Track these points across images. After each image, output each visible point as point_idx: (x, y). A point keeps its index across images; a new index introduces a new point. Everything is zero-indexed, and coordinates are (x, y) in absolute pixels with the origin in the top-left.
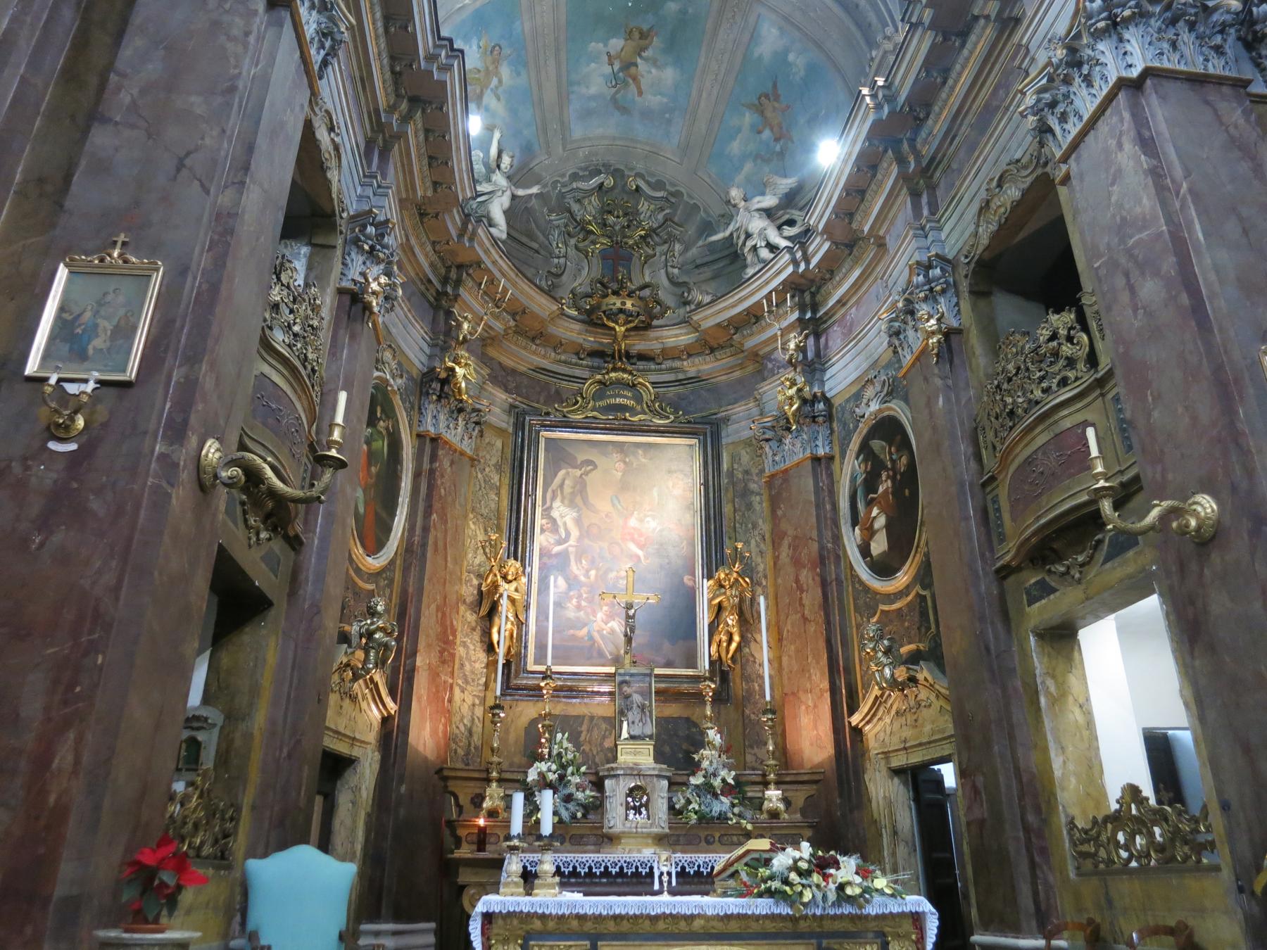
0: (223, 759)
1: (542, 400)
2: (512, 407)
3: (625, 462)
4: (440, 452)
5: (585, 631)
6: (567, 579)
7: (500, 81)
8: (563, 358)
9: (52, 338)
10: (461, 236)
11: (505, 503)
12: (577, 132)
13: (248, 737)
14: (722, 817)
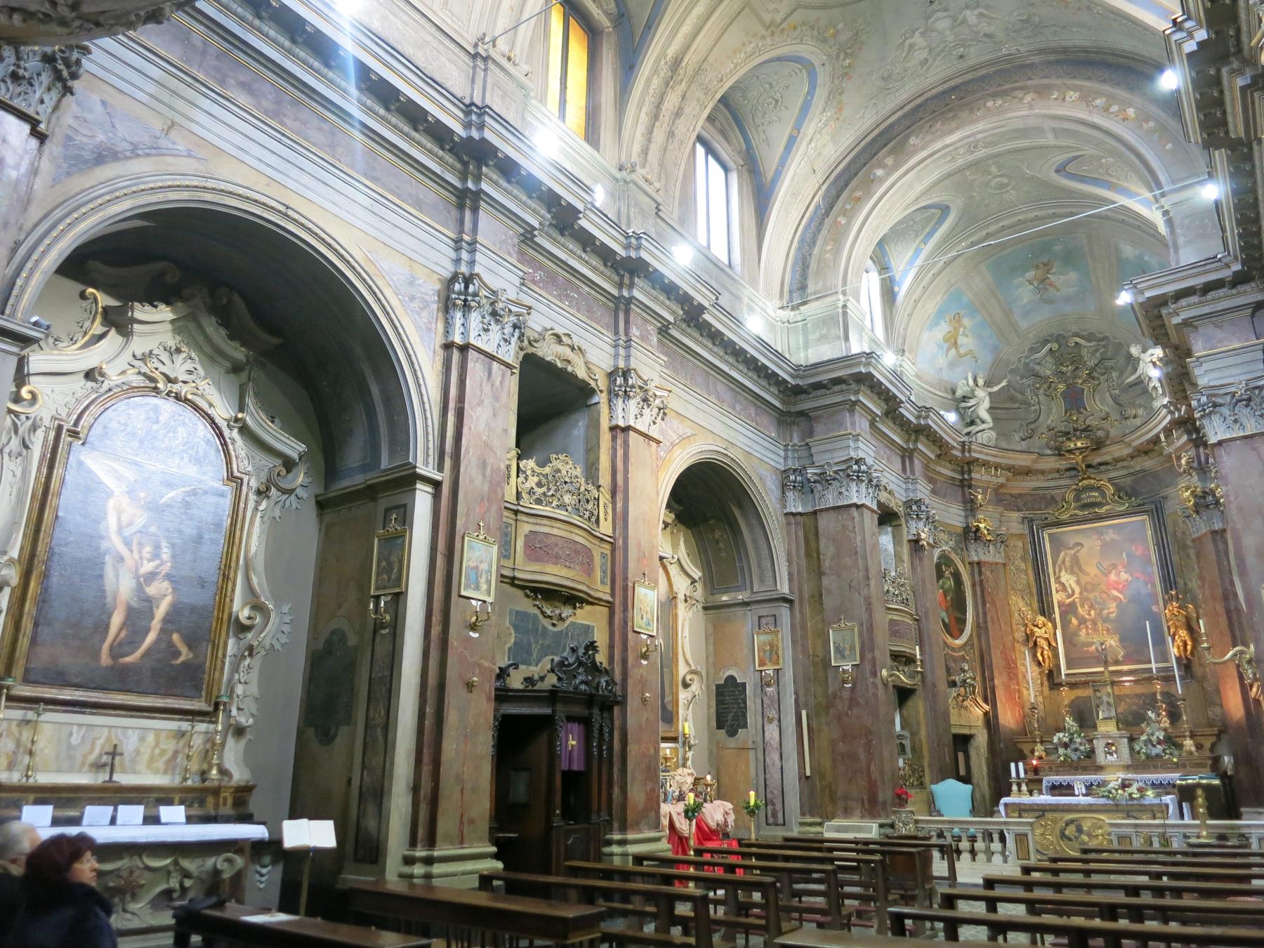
0: (913, 750)
1: (1043, 507)
2: (1024, 518)
3: (1099, 539)
4: (983, 569)
5: (1094, 647)
6: (1077, 618)
7: (965, 328)
8: (1050, 477)
9: (835, 653)
10: (963, 451)
11: (1032, 578)
12: (1024, 325)
13: (920, 740)
14: (1158, 756)
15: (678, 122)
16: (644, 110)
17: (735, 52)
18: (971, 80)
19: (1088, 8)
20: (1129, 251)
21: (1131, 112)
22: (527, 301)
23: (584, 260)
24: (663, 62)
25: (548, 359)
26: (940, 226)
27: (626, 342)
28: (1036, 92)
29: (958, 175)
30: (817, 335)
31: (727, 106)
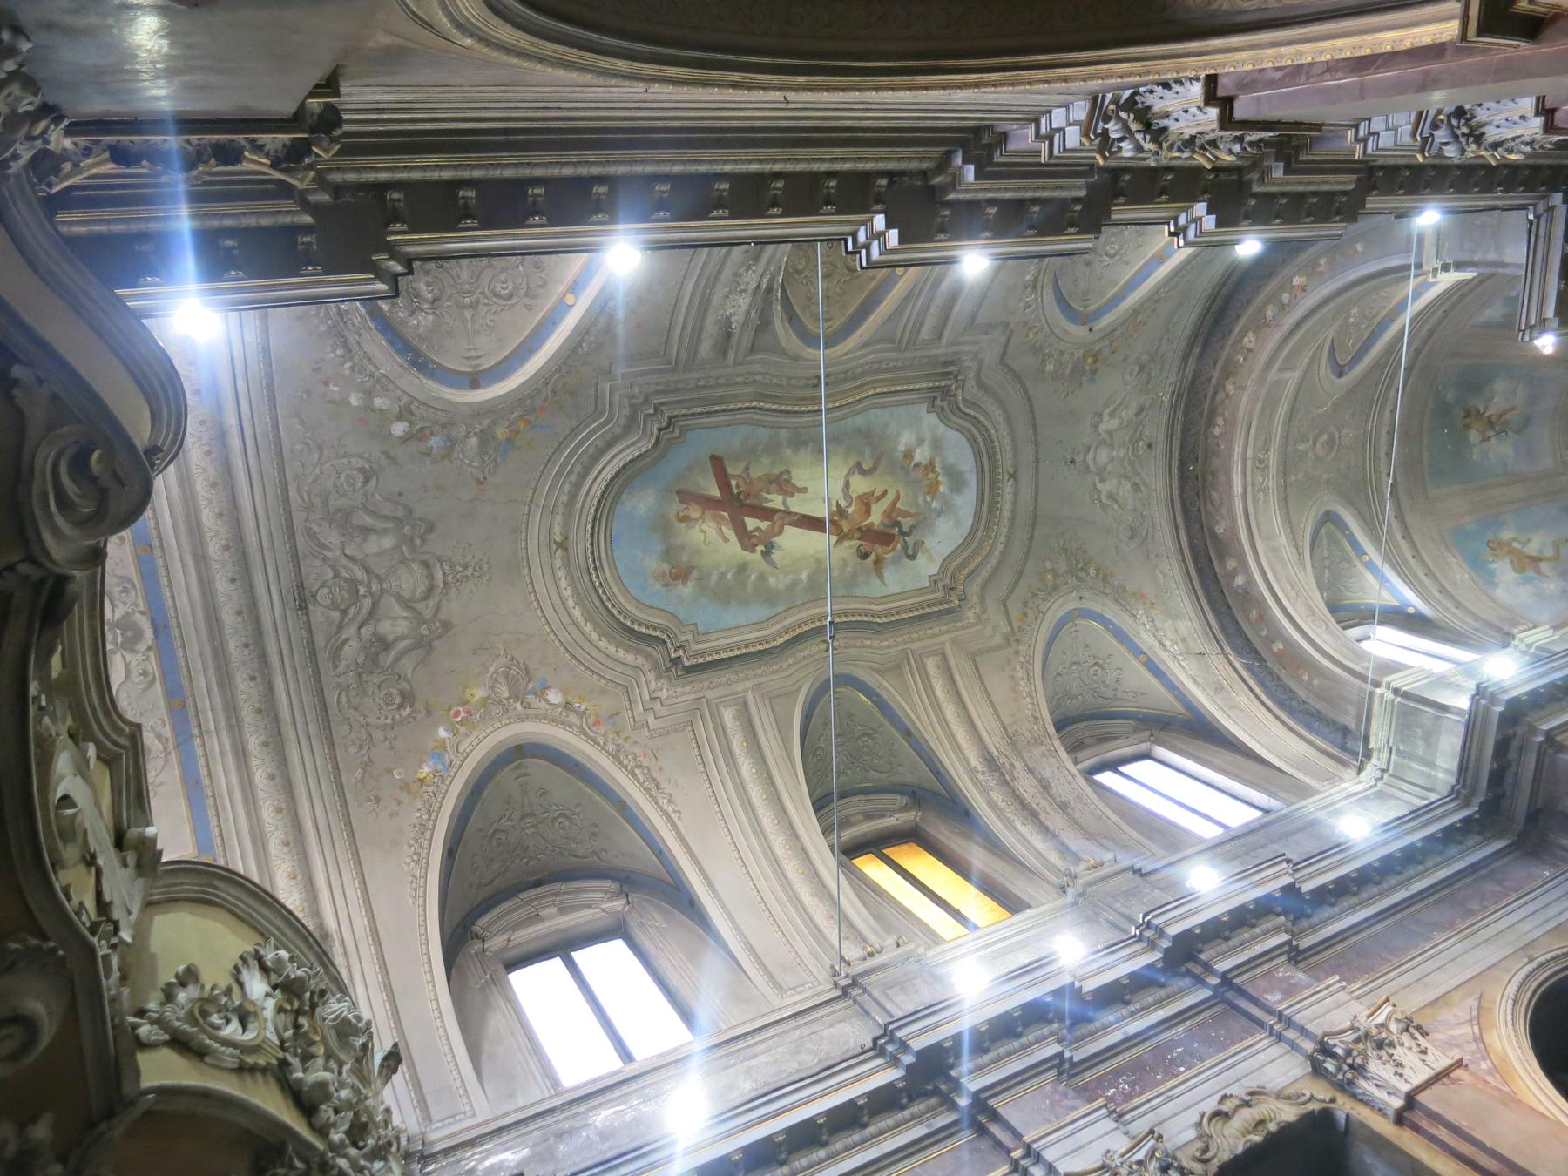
7: (1515, 540)
12: (1547, 462)
15: (1054, 791)
16: (1018, 825)
17: (1014, 690)
18: (1182, 447)
19: (1158, 301)
20: (1494, 313)
21: (1297, 281)
22: (1140, 1126)
23: (1138, 1011)
24: (980, 777)
25: (1240, 1150)
26: (1348, 529)
27: (1280, 1020)
28: (1227, 378)
29: (1289, 490)
30: (1420, 743)
31: (1074, 721)
